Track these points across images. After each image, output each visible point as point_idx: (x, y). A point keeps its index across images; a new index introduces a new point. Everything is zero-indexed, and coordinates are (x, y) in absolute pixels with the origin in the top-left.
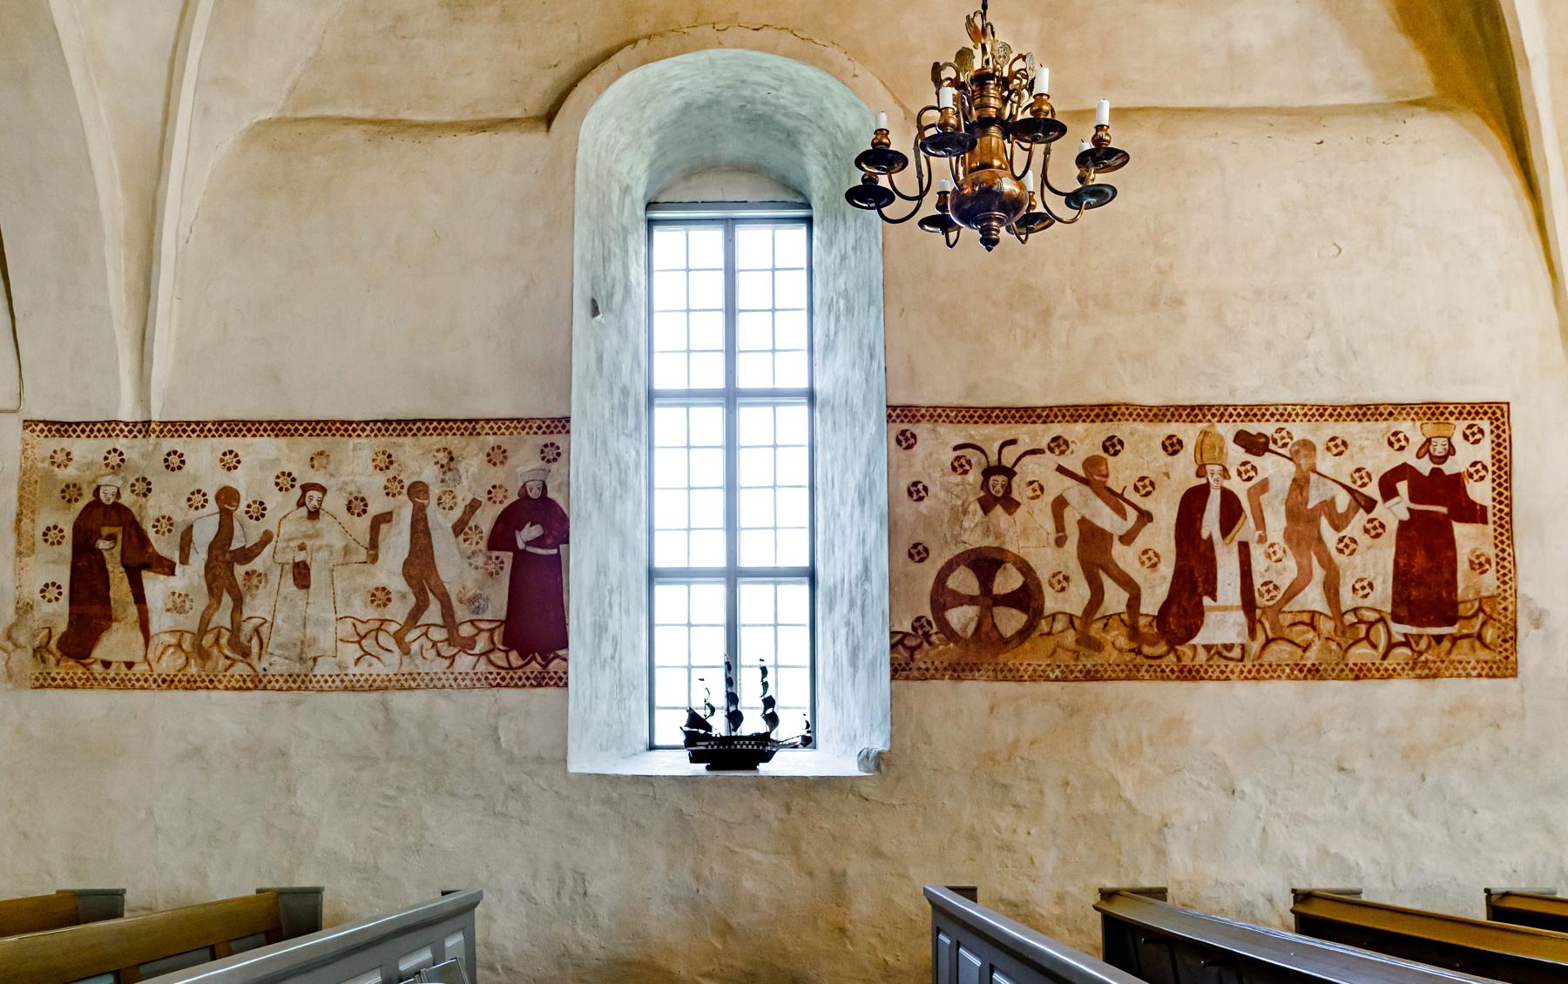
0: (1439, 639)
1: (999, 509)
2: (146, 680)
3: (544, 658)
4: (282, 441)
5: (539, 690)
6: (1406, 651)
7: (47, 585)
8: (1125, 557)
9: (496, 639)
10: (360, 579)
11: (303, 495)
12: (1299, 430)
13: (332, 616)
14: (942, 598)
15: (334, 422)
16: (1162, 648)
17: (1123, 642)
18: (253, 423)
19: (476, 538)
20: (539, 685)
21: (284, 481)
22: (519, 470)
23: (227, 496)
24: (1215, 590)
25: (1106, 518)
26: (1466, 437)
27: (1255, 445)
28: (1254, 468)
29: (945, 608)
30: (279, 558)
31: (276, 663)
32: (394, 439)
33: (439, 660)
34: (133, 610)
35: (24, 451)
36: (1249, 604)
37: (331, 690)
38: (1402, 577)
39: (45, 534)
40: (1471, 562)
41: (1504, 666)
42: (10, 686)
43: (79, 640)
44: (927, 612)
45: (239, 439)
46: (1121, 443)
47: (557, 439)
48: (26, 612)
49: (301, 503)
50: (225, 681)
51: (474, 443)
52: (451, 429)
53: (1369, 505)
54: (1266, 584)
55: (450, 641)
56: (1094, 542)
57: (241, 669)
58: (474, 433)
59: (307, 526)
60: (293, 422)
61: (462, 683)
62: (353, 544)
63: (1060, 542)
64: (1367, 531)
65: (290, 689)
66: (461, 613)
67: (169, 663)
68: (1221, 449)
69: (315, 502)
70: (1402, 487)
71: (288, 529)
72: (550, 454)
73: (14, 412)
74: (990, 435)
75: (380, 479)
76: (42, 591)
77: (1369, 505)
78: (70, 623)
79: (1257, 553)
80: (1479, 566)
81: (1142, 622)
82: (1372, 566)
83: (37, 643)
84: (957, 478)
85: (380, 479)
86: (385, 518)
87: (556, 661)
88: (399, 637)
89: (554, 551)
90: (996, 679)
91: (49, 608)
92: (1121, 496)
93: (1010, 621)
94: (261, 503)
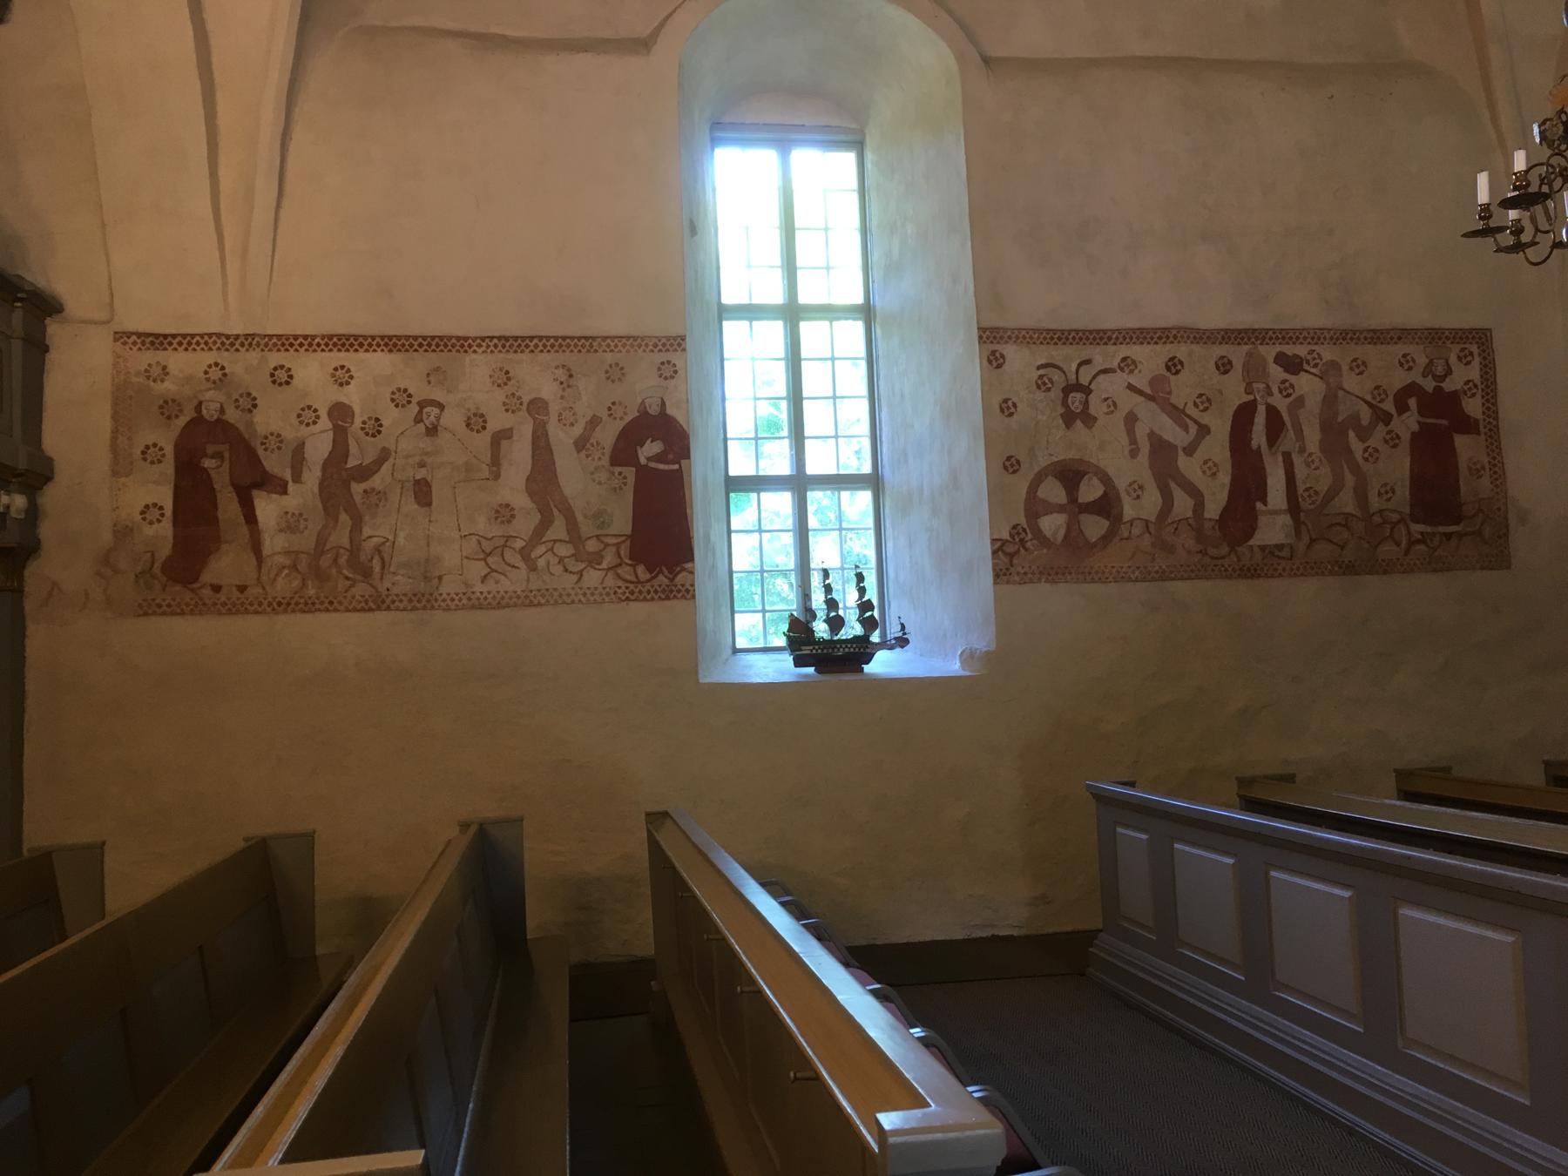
0: (1448, 536)
1: (1079, 423)
4: (396, 357)
6: (1422, 547)
8: (1189, 467)
11: (420, 412)
12: (1327, 353)
13: (456, 534)
14: (1035, 507)
15: (450, 338)
16: (1225, 550)
17: (1191, 544)
18: (365, 337)
20: (668, 598)
21: (402, 399)
23: (340, 413)
24: (1265, 495)
25: (1172, 432)
26: (1460, 359)
27: (1292, 365)
28: (1292, 386)
29: (1038, 516)
32: (511, 356)
35: (115, 365)
36: (1294, 507)
37: (457, 608)
38: (1418, 482)
39: (143, 453)
40: (1470, 469)
41: (1500, 560)
44: (1023, 521)
45: (352, 354)
46: (1181, 363)
47: (674, 357)
49: (418, 420)
52: (568, 346)
53: (1387, 419)
54: (1307, 490)
56: (1162, 452)
57: (361, 590)
60: (407, 337)
63: (1134, 454)
64: (1386, 442)
65: (414, 609)
66: (586, 528)
67: (283, 586)
68: (1264, 368)
70: (1412, 402)
72: (667, 372)
73: (103, 323)
74: (1067, 357)
75: (500, 395)
76: (142, 513)
77: (1387, 419)
78: (175, 545)
79: (1298, 461)
80: (1476, 471)
81: (1207, 525)
82: (1396, 469)
83: (139, 569)
84: (1040, 395)
85: (500, 395)
86: (504, 435)
88: (525, 554)
89: (676, 467)
90: (1085, 581)
91: (150, 531)
92: (1183, 412)
93: (1094, 527)
94: (377, 420)
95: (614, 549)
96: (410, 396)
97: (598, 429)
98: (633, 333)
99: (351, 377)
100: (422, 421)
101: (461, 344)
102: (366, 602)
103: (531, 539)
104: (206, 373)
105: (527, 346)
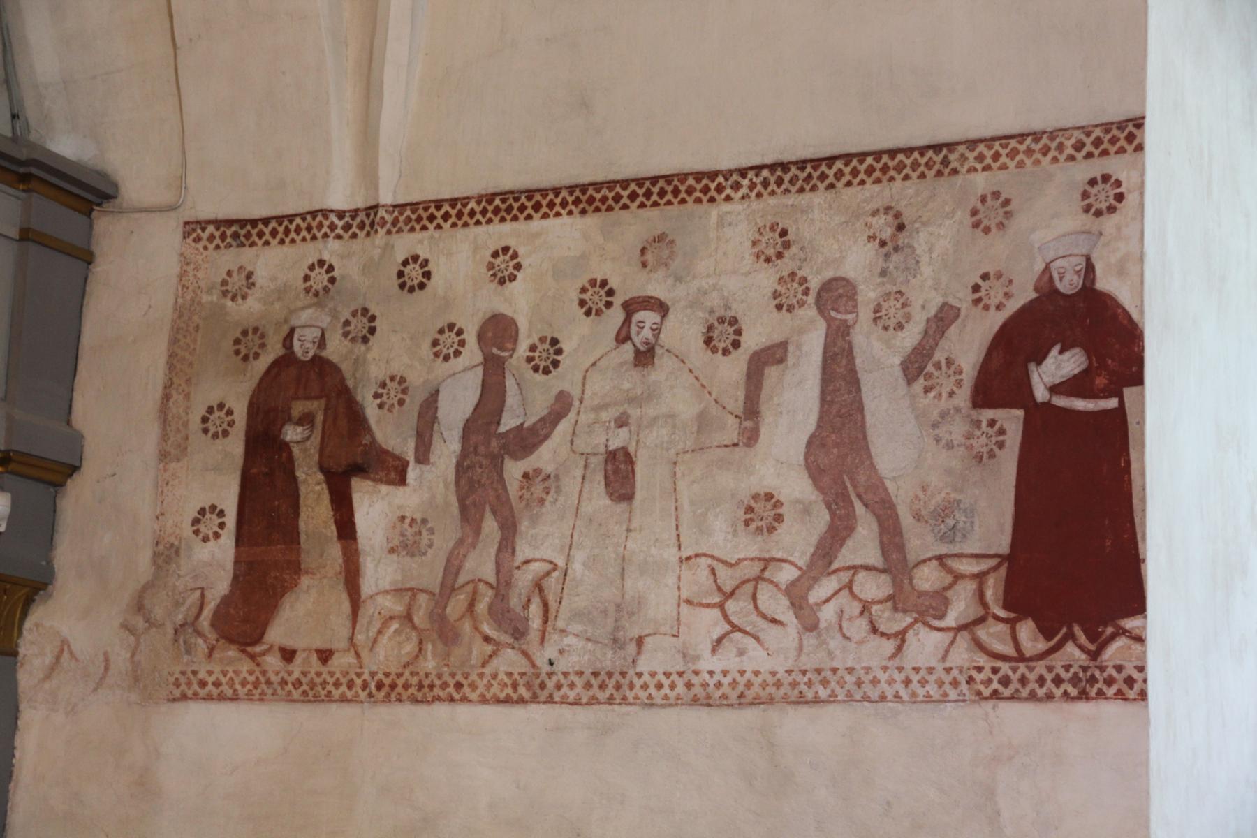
2: (350, 685)
3: (1093, 636)
4: (592, 220)
5: (1083, 707)
7: (202, 511)
9: (989, 594)
10: (725, 479)
13: (671, 554)
15: (683, 177)
18: (543, 192)
19: (948, 385)
20: (1083, 696)
21: (596, 298)
22: (1037, 237)
23: (498, 331)
30: (581, 445)
31: (570, 650)
32: (792, 199)
33: (876, 641)
34: (335, 551)
35: (182, 274)
37: (668, 703)
39: (205, 420)
42: (134, 697)
43: (246, 614)
45: (521, 225)
47: (1116, 166)
48: (168, 560)
49: (623, 337)
50: (482, 684)
51: (945, 189)
52: (900, 168)
55: (895, 601)
57: (509, 661)
58: (946, 170)
59: (631, 381)
60: (611, 184)
61: (920, 690)
62: (715, 410)
65: (593, 701)
66: (920, 542)
67: (388, 653)
69: (647, 333)
71: (599, 386)
72: (1101, 198)
73: (171, 208)
75: (766, 279)
76: (196, 522)
78: (235, 577)
83: (180, 618)
85: (766, 279)
86: (773, 355)
87: (1121, 642)
88: (796, 596)
89: (1112, 403)
95: (971, 586)
96: (611, 293)
97: (953, 330)
98: (1037, 126)
99: (518, 267)
100: (628, 338)
101: (703, 186)
102: (515, 686)
103: (812, 564)
104: (307, 278)
105: (823, 177)
